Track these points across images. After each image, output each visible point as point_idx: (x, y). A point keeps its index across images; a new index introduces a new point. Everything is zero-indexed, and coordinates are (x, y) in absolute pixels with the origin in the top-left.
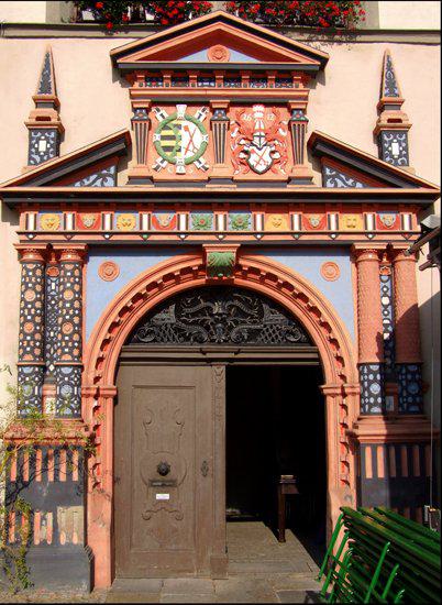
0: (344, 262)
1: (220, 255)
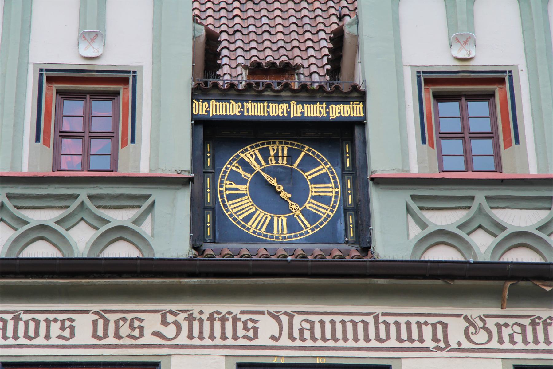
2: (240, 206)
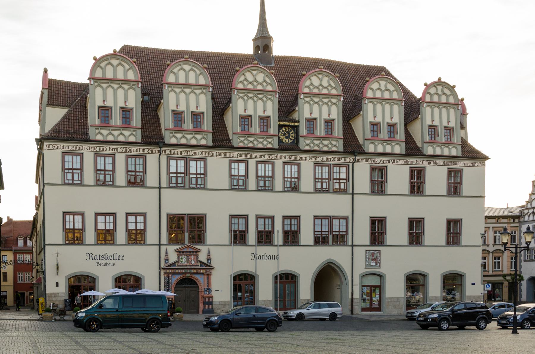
0: (202, 276)
1: (188, 275)
2: (282, 138)
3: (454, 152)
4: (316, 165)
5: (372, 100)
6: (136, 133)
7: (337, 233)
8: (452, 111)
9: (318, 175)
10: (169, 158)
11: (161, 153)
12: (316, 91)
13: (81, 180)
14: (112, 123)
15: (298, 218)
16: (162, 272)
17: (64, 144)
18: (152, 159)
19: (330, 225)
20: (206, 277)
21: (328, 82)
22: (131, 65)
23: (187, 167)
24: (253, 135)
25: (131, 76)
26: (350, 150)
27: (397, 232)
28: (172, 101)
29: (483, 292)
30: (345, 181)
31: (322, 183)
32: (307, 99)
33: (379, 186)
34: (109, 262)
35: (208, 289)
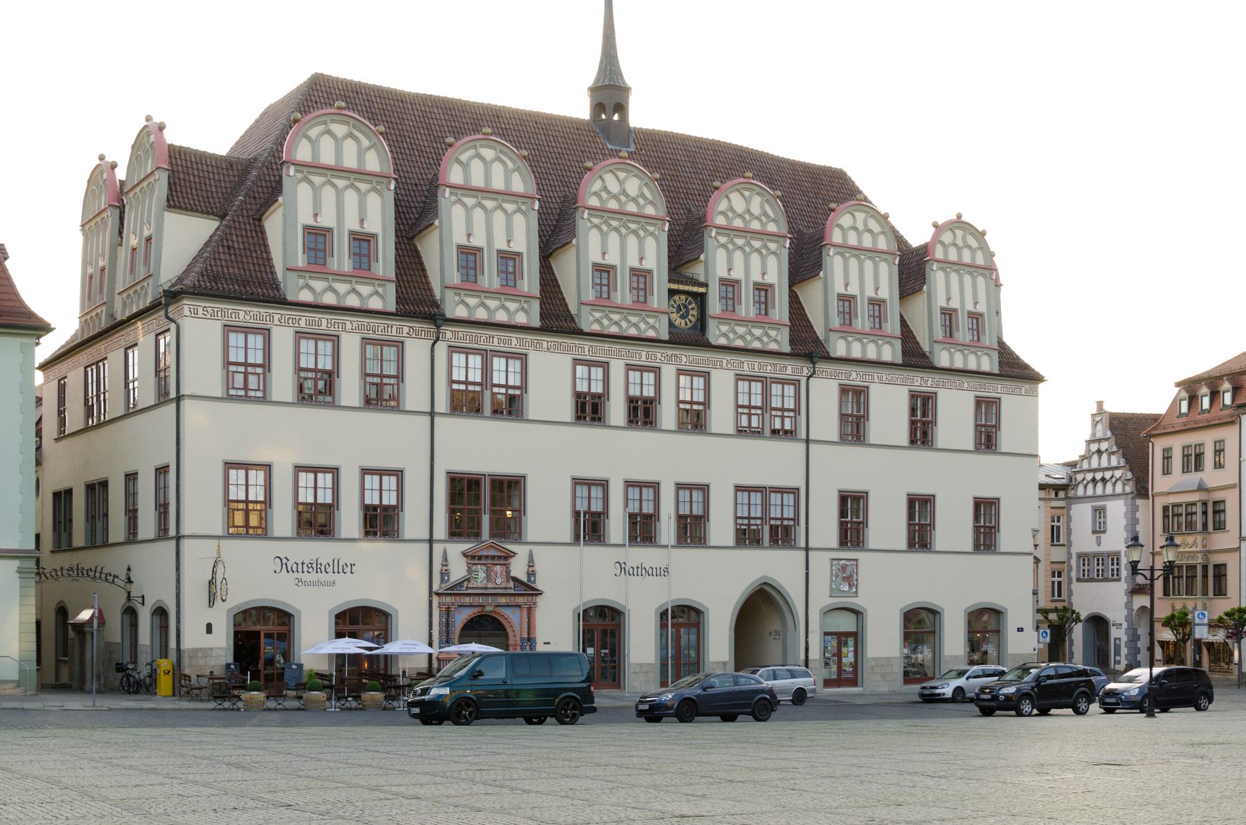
0: (518, 610)
1: (489, 609)
3: (986, 365)
4: (739, 377)
5: (841, 250)
6: (385, 291)
7: (779, 523)
8: (981, 281)
9: (743, 400)
10: (453, 349)
11: (438, 339)
12: (738, 223)
13: (264, 391)
14: (333, 264)
15: (704, 489)
16: (436, 600)
17: (229, 307)
18: (417, 350)
19: (765, 505)
20: (525, 613)
21: (762, 207)
22: (374, 140)
23: (486, 369)
24: (619, 308)
25: (373, 163)
26: (802, 349)
27: (887, 523)
28: (459, 223)
29: (1036, 645)
30: (792, 414)
31: (750, 415)
32: (723, 240)
33: (854, 428)
34: (323, 577)
35: (529, 639)
